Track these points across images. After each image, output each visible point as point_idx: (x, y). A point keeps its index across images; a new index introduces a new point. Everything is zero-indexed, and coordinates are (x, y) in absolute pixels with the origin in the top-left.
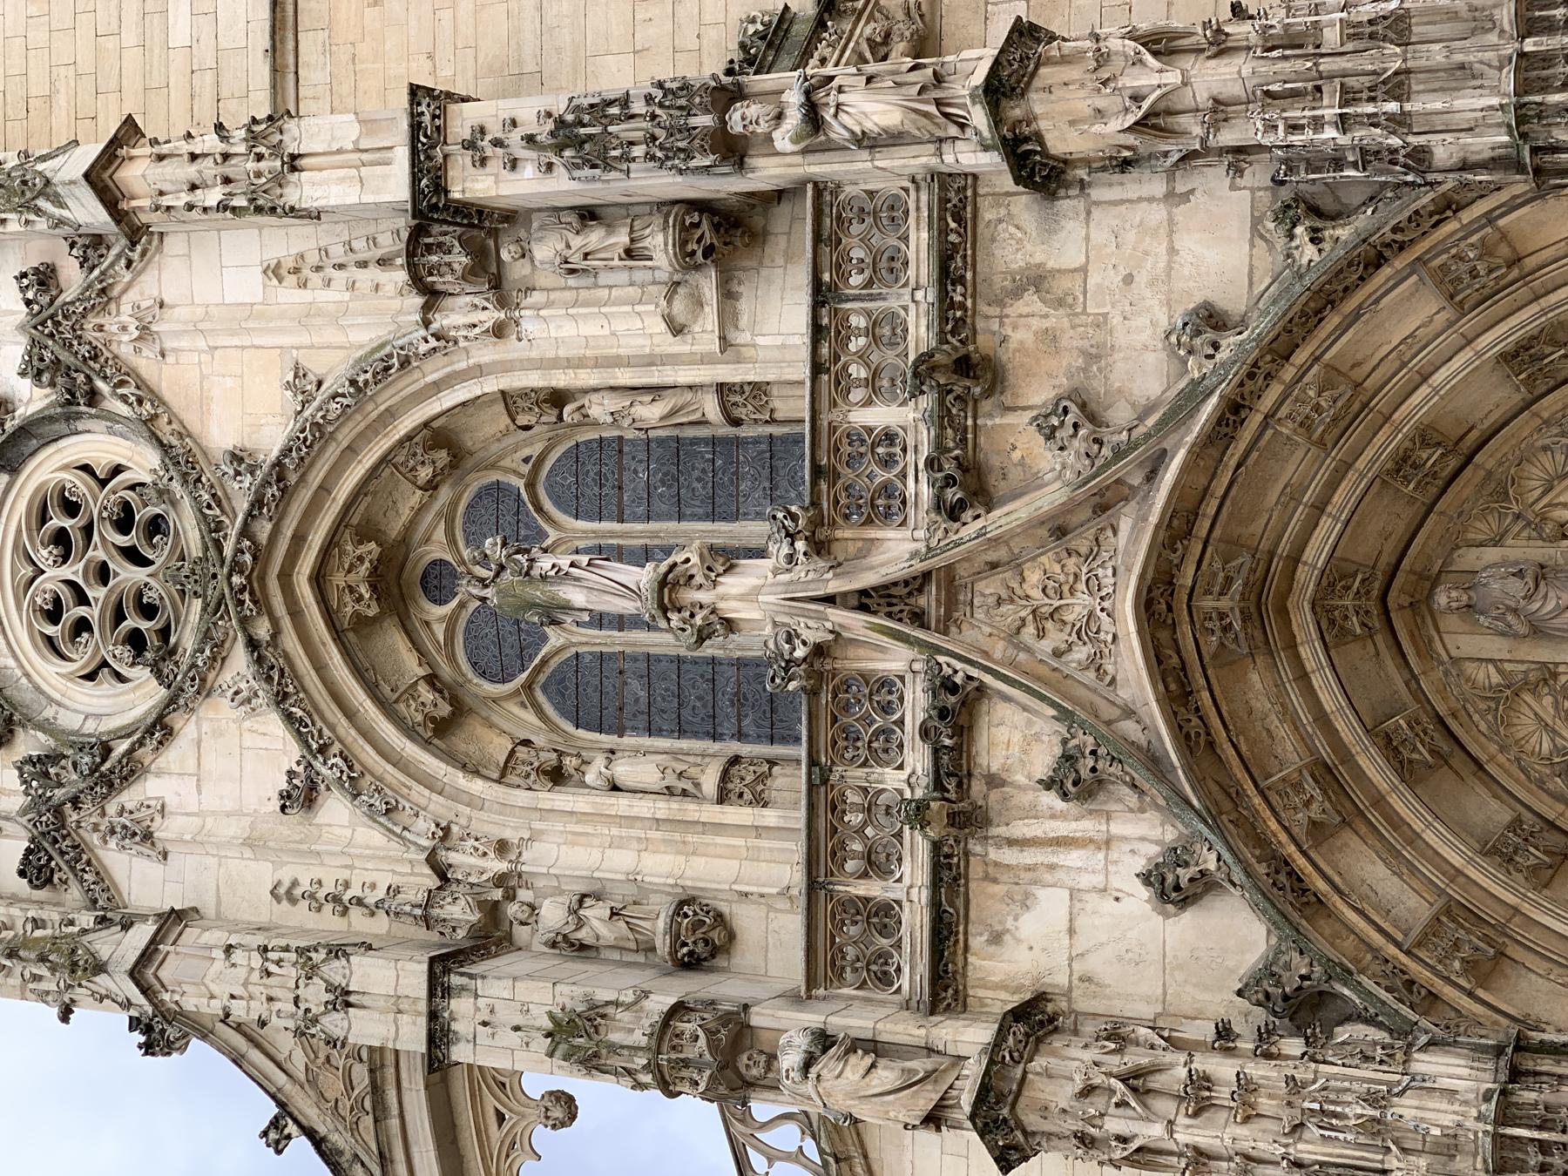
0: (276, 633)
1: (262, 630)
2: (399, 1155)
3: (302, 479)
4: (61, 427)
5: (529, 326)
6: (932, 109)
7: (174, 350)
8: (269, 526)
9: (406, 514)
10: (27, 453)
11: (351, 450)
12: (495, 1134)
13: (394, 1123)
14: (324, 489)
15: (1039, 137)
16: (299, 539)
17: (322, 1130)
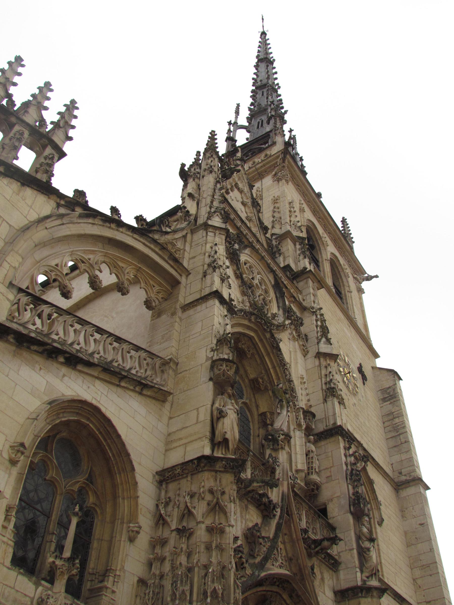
0: (250, 320)
1: (253, 318)
2: (160, 253)
3: (273, 353)
4: (281, 305)
5: (298, 433)
6: (374, 572)
7: (290, 343)
8: (267, 337)
9: (248, 368)
10: (277, 293)
11: (274, 367)
12: (152, 282)
13: (166, 258)
14: (268, 354)
15: (365, 597)
16: (261, 340)
17: (166, 236)
